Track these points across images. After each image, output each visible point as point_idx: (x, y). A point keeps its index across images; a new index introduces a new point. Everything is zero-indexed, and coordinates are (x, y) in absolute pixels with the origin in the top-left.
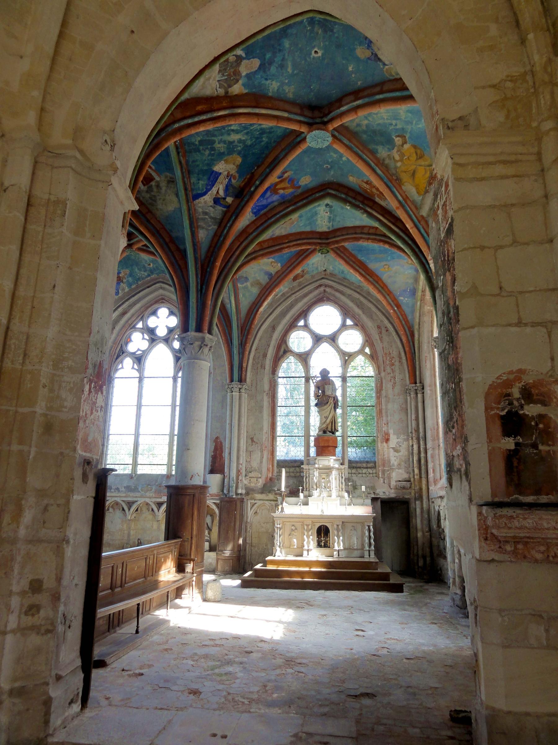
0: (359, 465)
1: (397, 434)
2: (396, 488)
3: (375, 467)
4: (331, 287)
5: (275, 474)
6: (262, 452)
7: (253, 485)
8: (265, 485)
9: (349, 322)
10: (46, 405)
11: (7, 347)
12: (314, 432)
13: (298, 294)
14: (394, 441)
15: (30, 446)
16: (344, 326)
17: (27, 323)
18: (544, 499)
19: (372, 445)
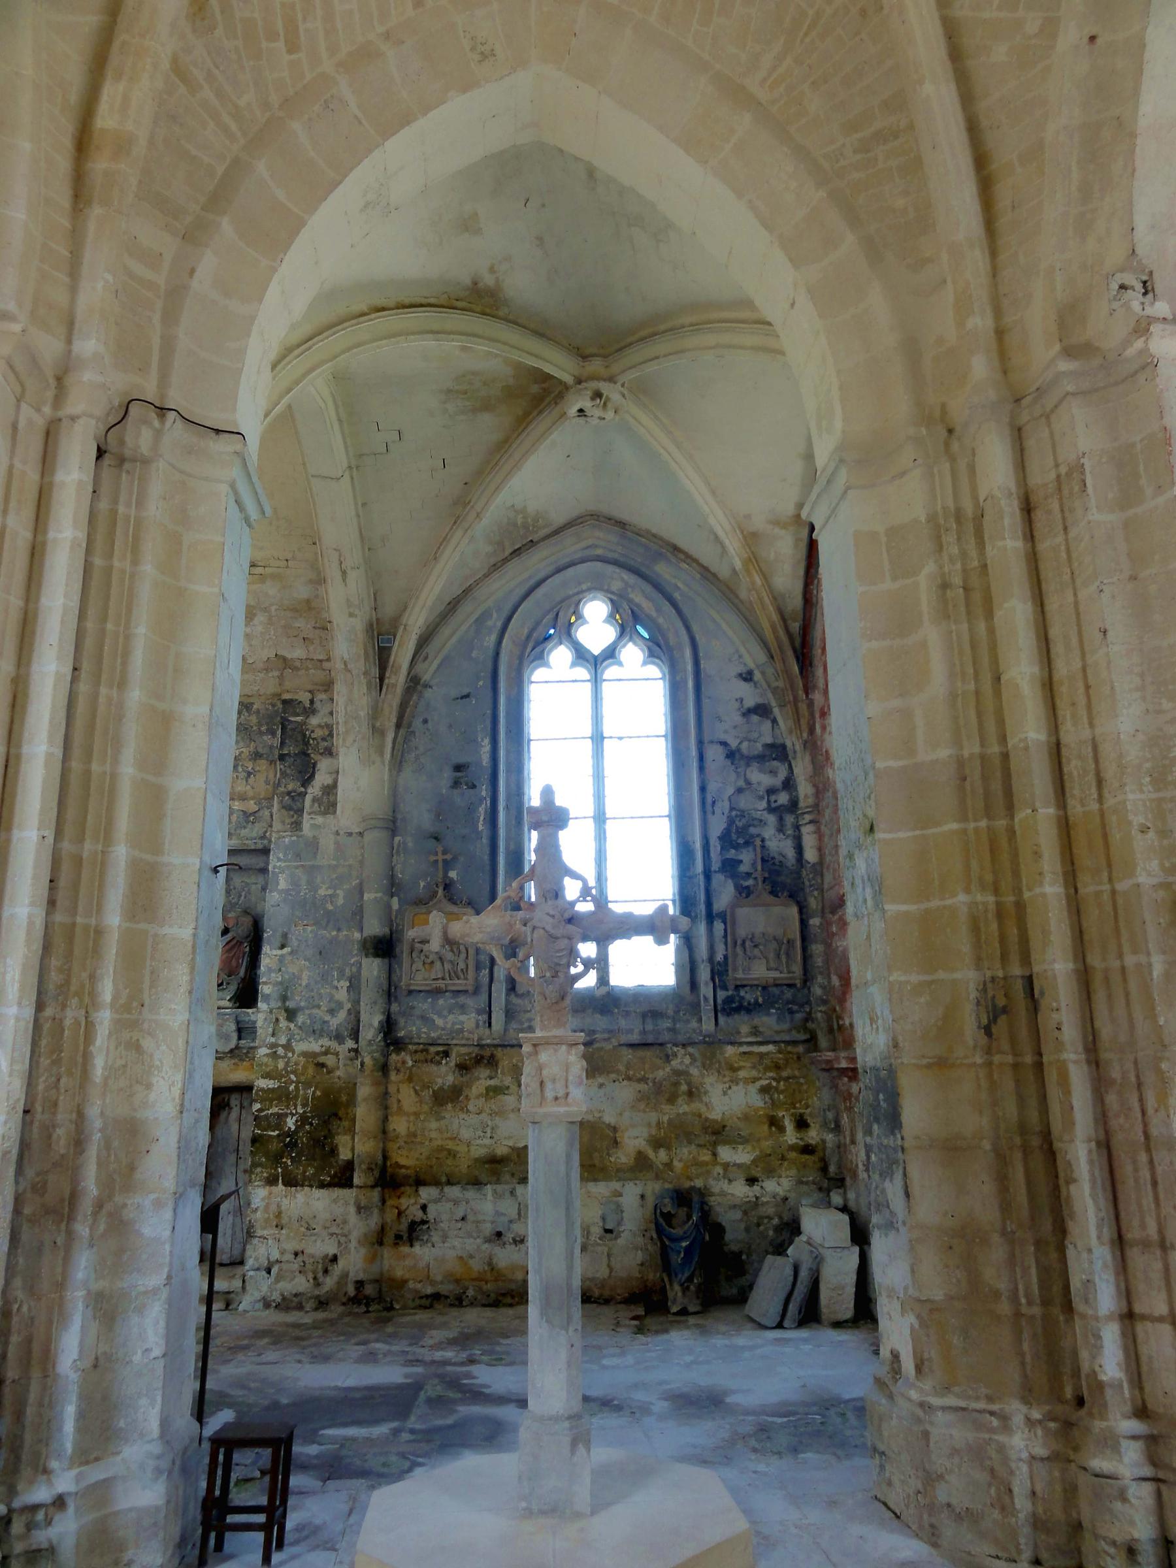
10: (1162, 865)
11: (1066, 777)
15: (1149, 954)
17: (1085, 720)
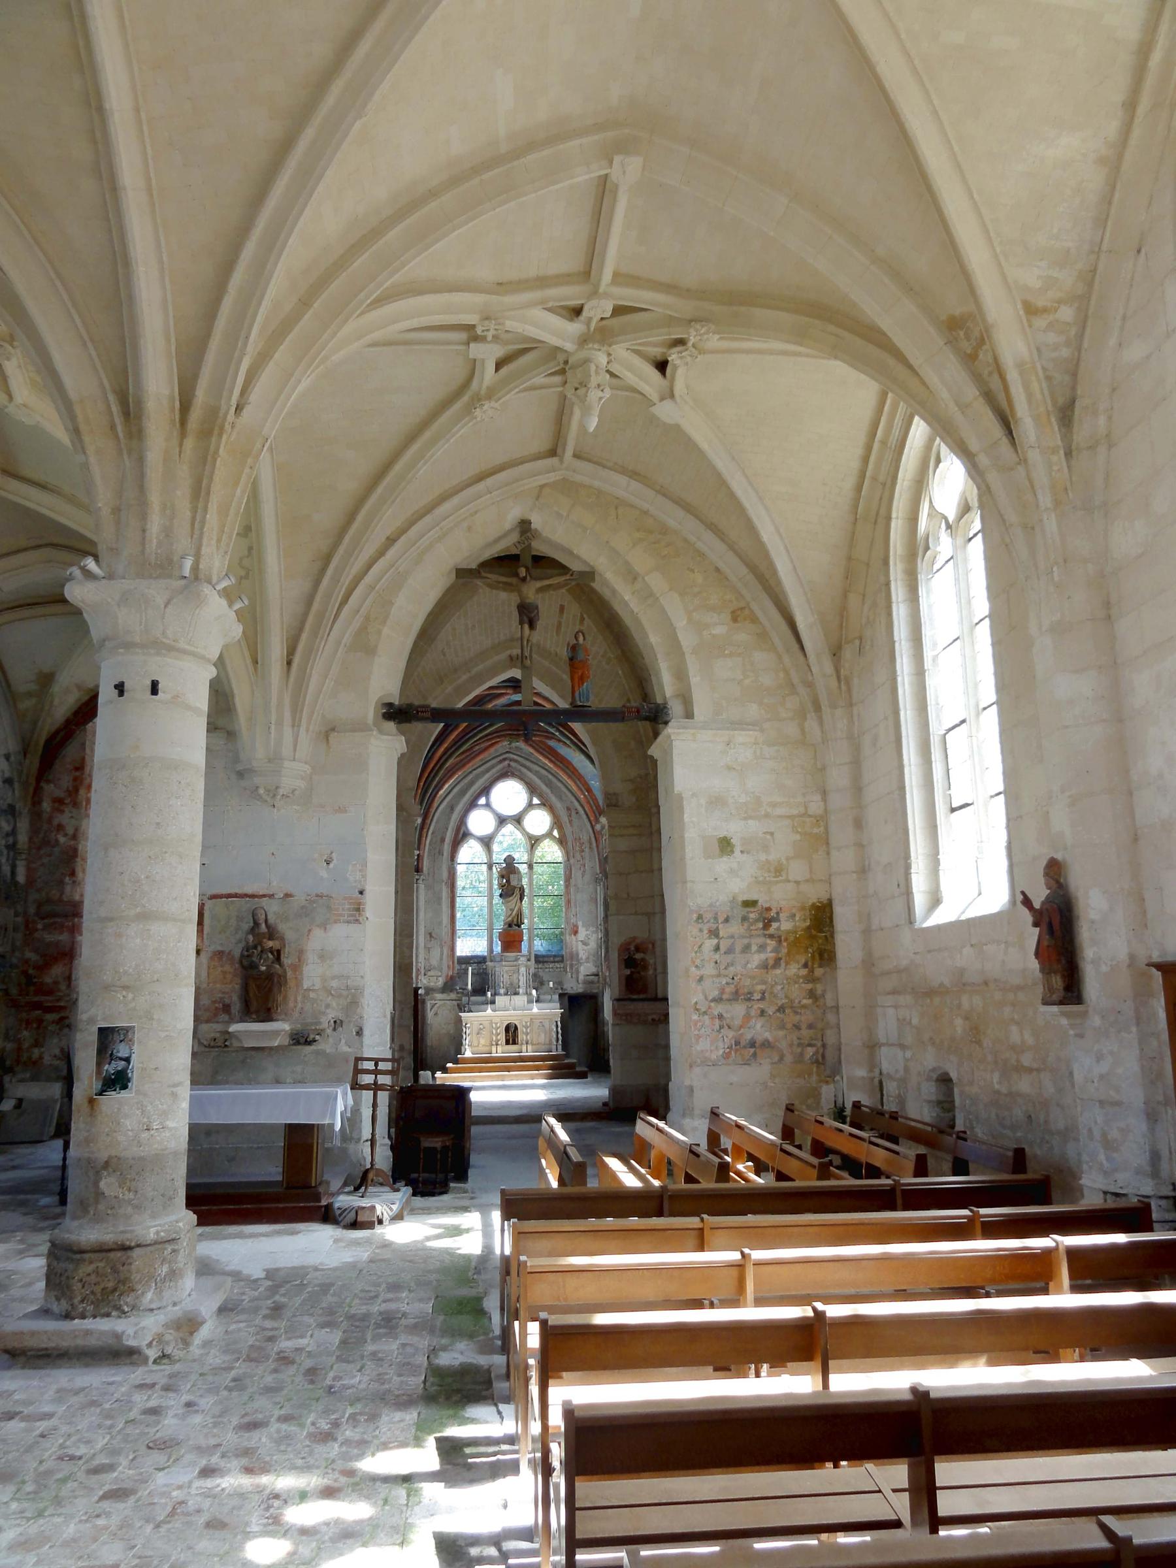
0: (546, 959)
1: (586, 926)
2: (585, 982)
3: (562, 961)
4: (516, 761)
5: (456, 972)
6: (442, 947)
7: (432, 984)
8: (445, 984)
9: (536, 801)
12: (499, 926)
13: (479, 770)
14: (582, 933)
16: (530, 806)
18: (641, 996)
19: (559, 939)
